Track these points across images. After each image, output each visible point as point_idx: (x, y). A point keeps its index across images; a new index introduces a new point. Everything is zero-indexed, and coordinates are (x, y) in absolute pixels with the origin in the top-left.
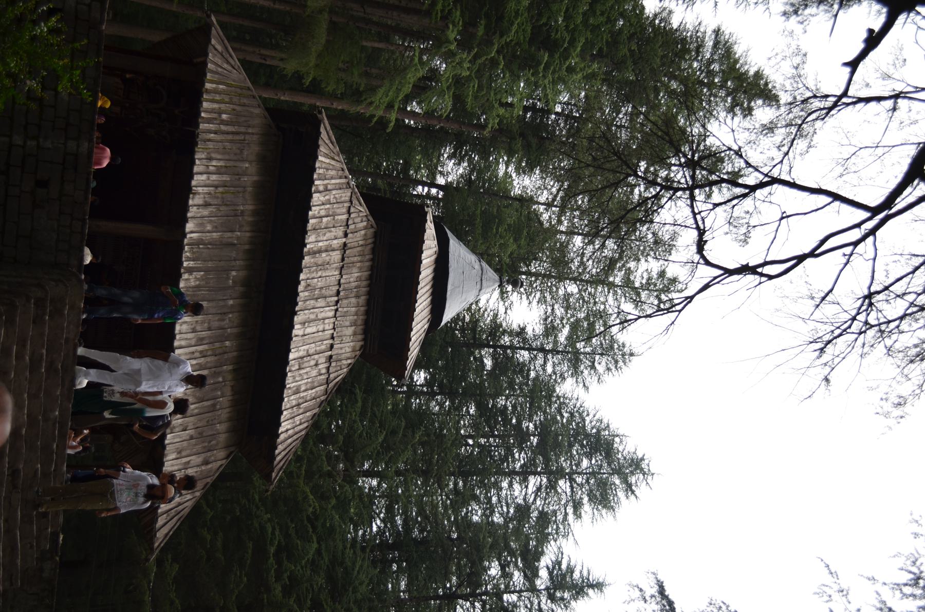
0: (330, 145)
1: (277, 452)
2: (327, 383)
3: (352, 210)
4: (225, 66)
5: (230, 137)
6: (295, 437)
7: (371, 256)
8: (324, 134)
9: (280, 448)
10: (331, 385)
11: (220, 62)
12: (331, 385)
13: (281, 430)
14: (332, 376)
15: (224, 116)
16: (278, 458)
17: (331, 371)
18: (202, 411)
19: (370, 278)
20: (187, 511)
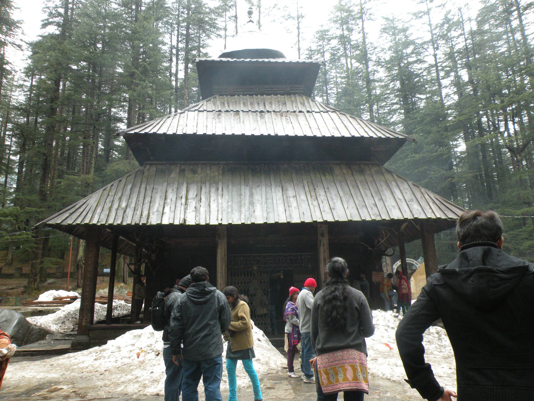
0: (146, 126)
1: (383, 137)
2: (327, 112)
3: (201, 109)
4: (81, 210)
5: (141, 199)
6: (370, 126)
7: (236, 96)
8: (137, 131)
9: (379, 135)
10: (328, 109)
11: (77, 214)
12: (328, 109)
13: (366, 135)
14: (322, 109)
15: (124, 205)
16: (388, 135)
17: (319, 111)
18: (359, 195)
19: (251, 95)
20: (438, 197)
